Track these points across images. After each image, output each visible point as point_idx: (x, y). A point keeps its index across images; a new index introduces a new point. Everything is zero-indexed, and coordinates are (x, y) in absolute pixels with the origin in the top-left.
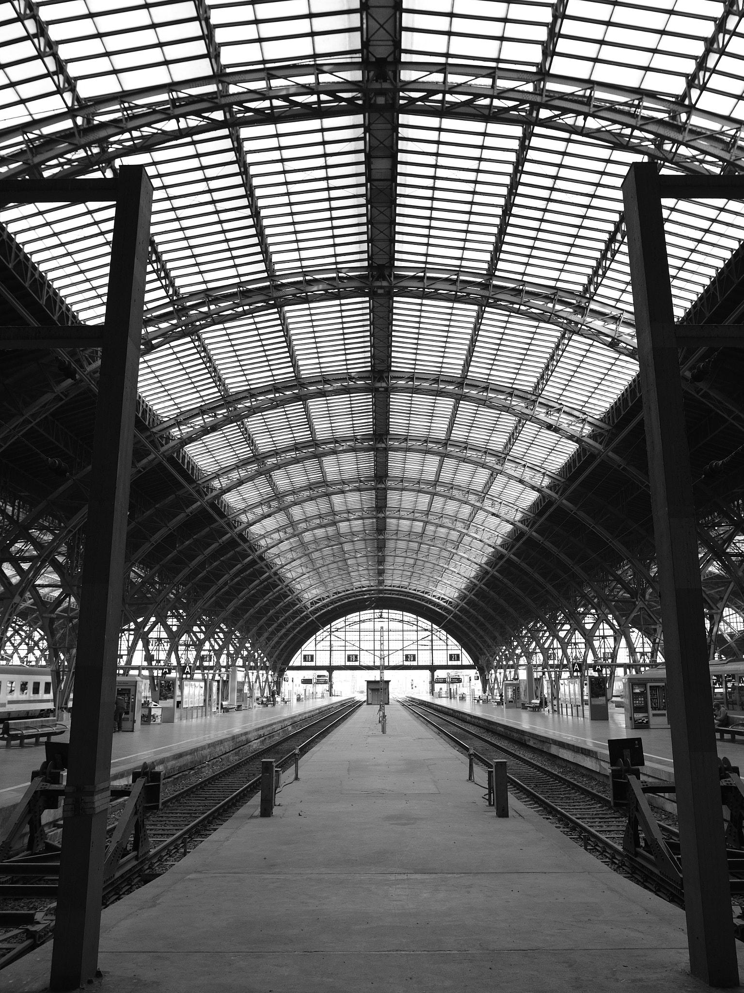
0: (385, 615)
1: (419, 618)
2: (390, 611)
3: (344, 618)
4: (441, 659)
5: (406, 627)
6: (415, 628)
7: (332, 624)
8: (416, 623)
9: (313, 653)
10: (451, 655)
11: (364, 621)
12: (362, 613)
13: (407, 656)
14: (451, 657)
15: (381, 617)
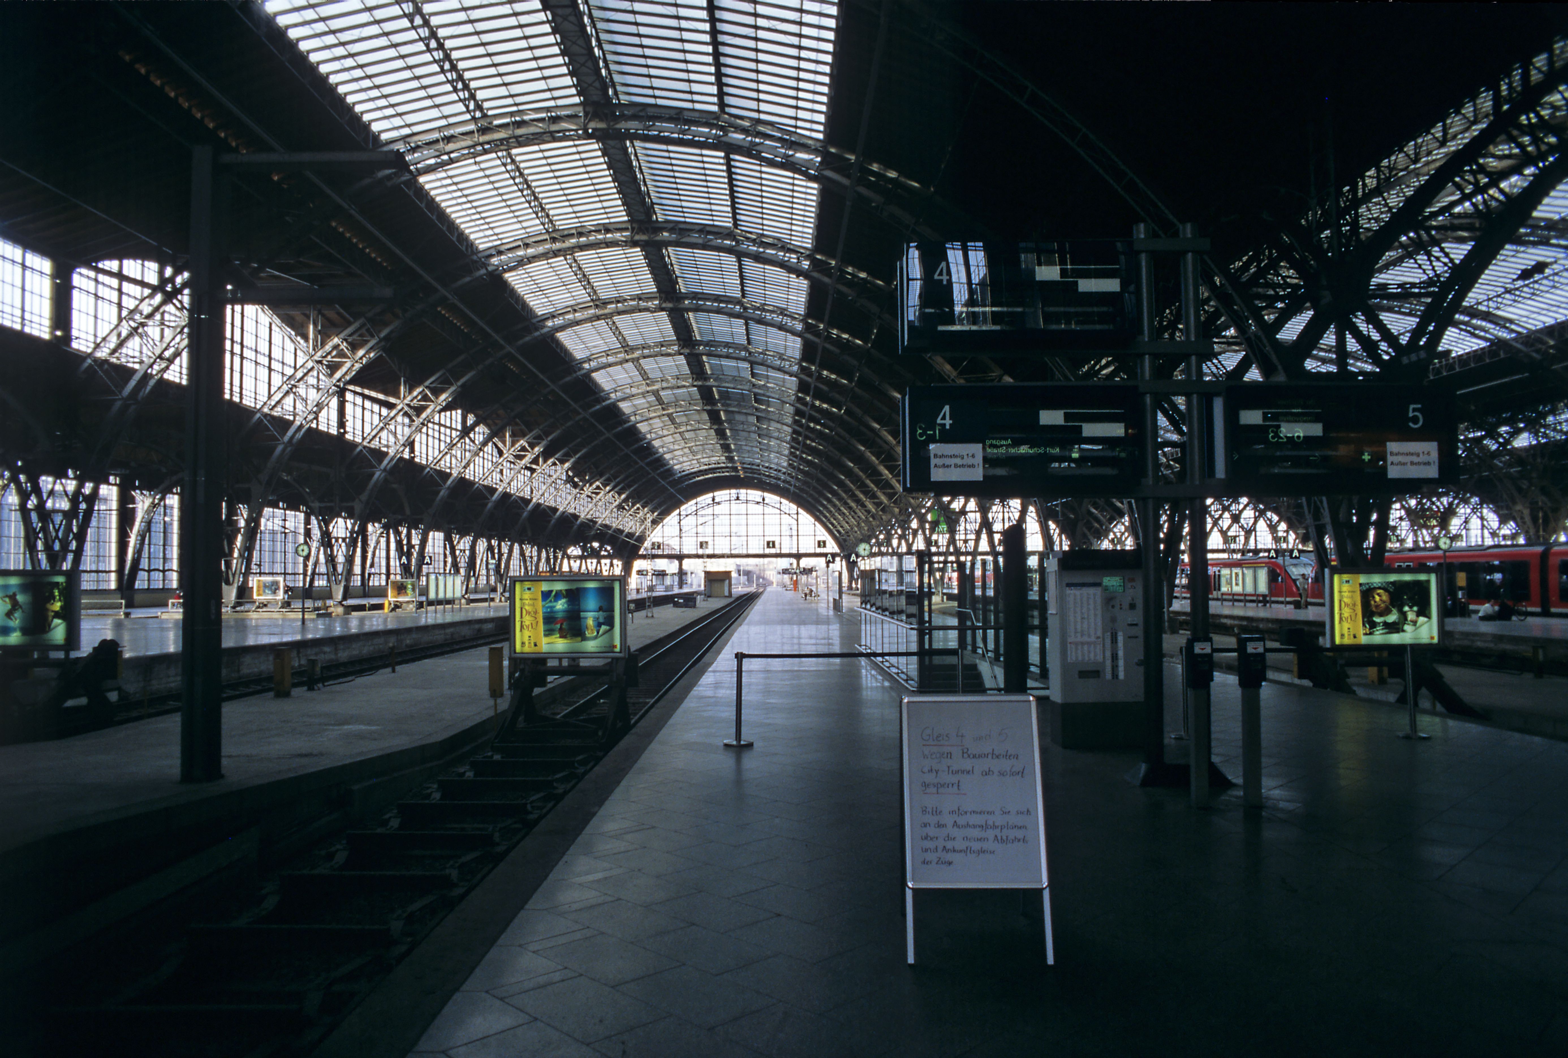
0: (742, 497)
1: (783, 500)
2: (749, 491)
3: (694, 501)
4: (808, 545)
5: (768, 510)
6: (778, 511)
7: (683, 508)
8: (778, 505)
9: (660, 540)
10: (819, 542)
11: (718, 503)
12: (716, 494)
13: (768, 543)
14: (822, 544)
15: (738, 498)
